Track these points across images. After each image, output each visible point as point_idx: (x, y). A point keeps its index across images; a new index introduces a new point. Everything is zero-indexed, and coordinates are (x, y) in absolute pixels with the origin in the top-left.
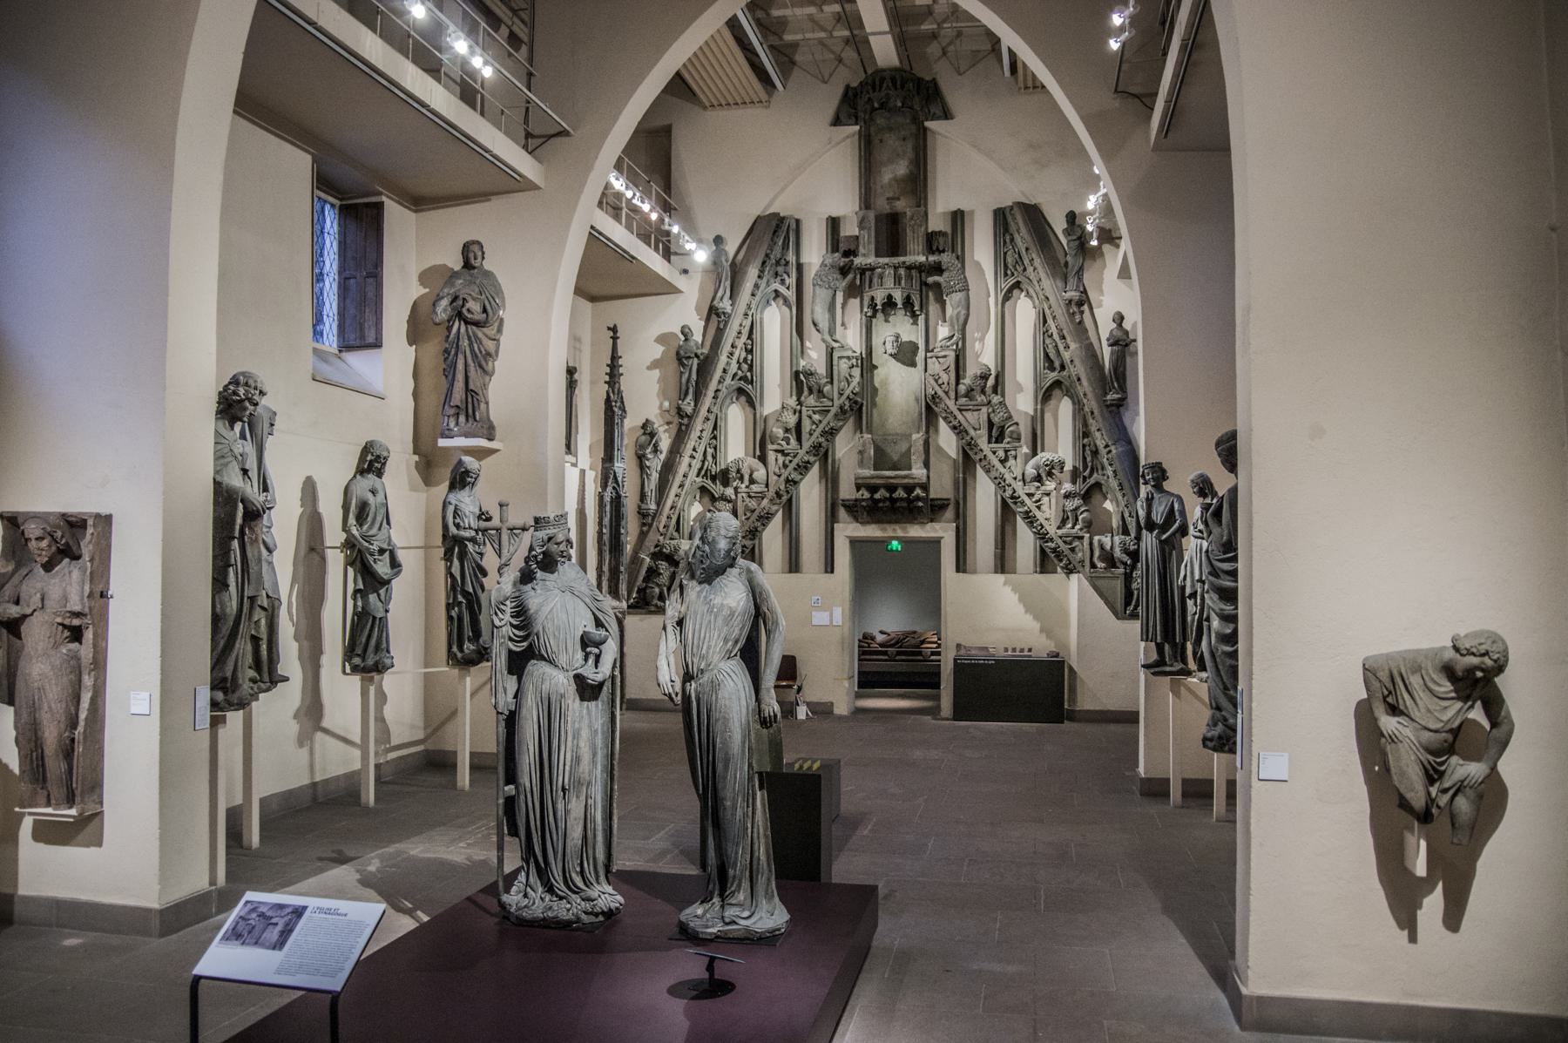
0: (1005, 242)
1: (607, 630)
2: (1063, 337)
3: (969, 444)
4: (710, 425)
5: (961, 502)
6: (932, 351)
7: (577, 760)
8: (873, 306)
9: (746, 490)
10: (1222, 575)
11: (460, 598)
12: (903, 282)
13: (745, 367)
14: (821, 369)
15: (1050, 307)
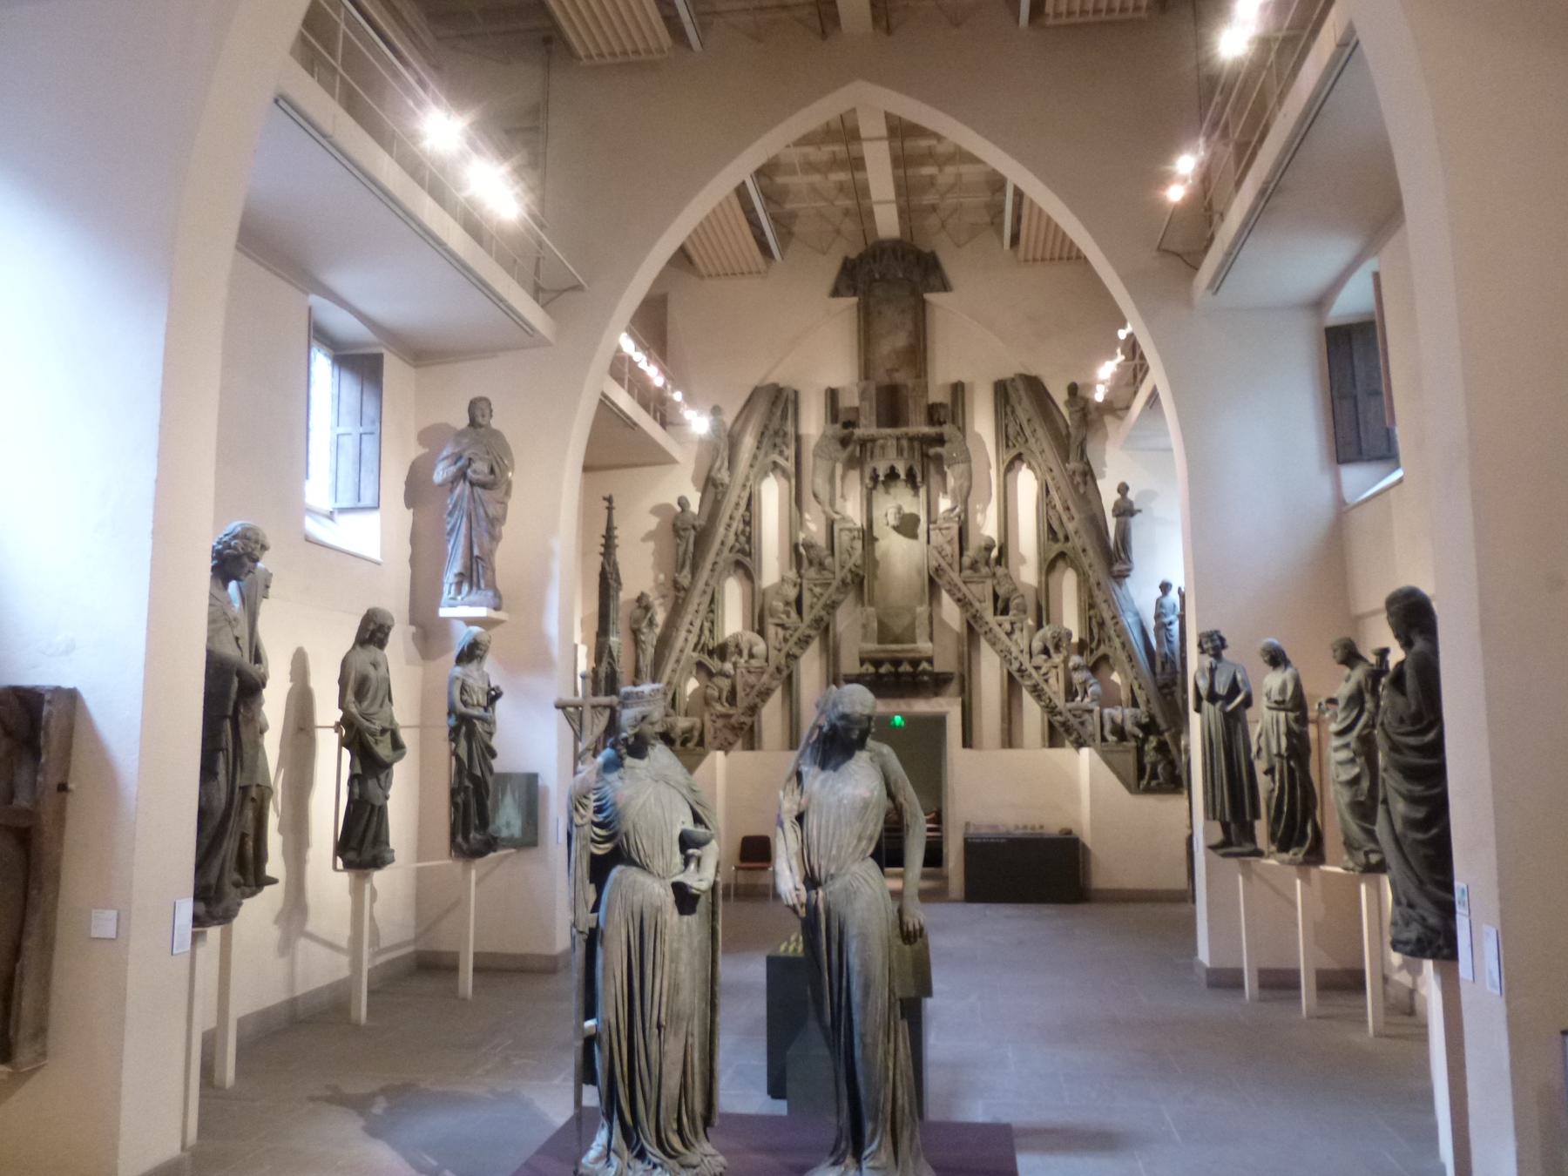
0: (1006, 414)
1: (707, 827)
2: (1068, 509)
3: (974, 617)
4: (707, 599)
5: (966, 675)
6: (935, 522)
7: (675, 988)
8: (875, 478)
10: (1406, 751)
11: (467, 783)
12: (906, 454)
13: (742, 539)
14: (821, 540)
15: (1053, 479)
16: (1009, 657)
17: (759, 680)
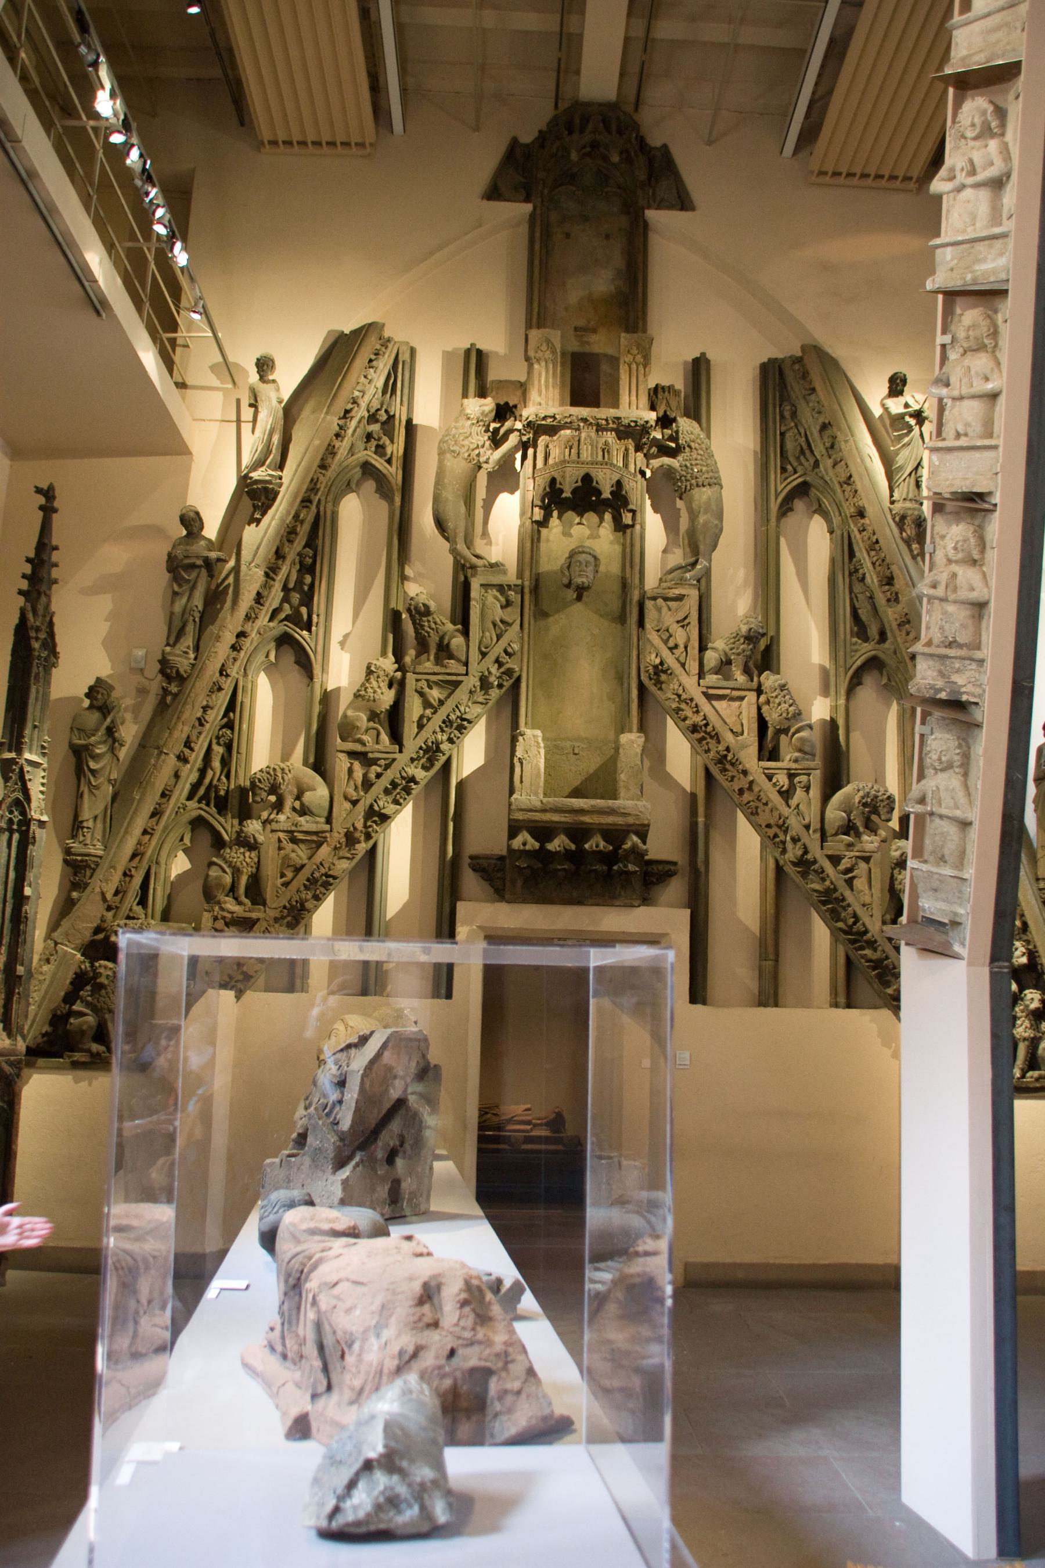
0: (782, 417)
3: (722, 760)
4: (222, 700)
9: (288, 826)
13: (296, 597)
16: (782, 837)
17: (309, 858)
